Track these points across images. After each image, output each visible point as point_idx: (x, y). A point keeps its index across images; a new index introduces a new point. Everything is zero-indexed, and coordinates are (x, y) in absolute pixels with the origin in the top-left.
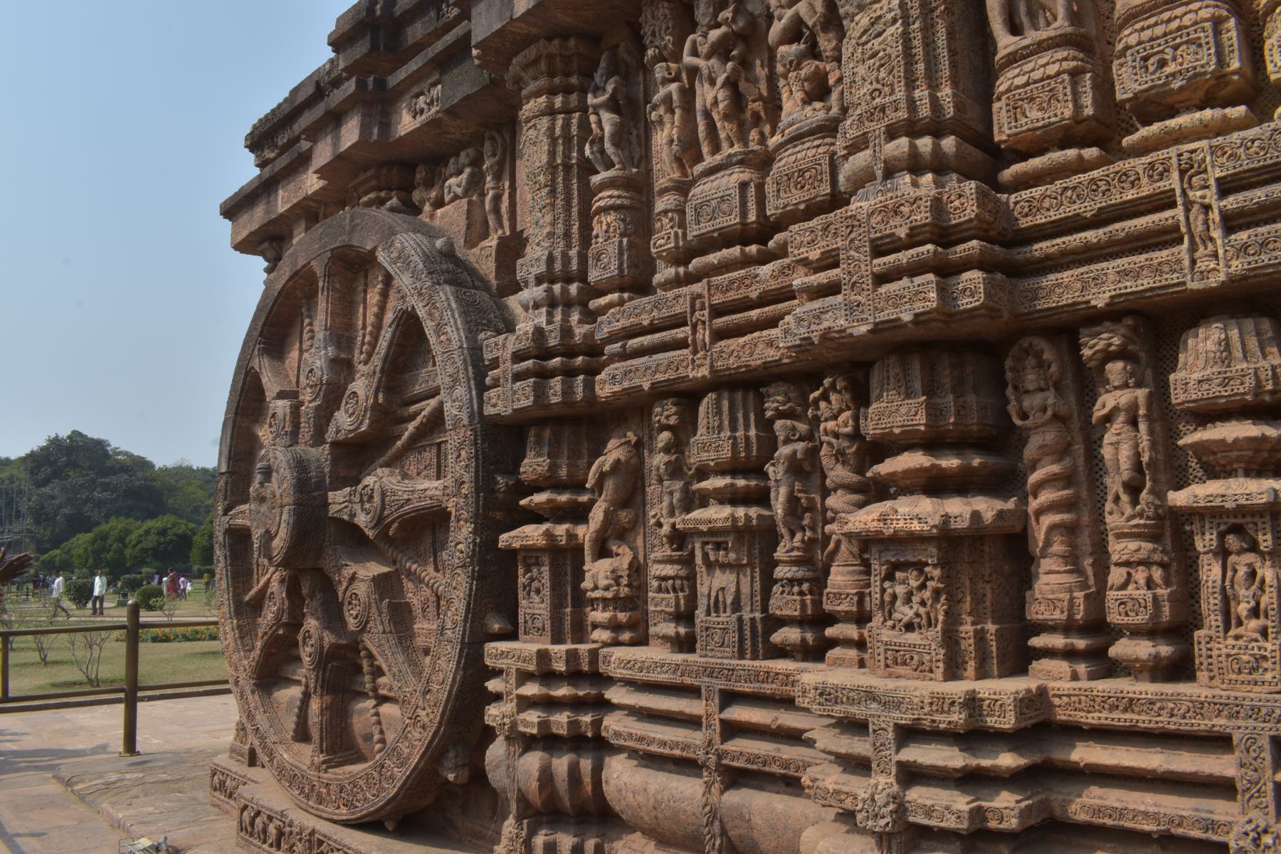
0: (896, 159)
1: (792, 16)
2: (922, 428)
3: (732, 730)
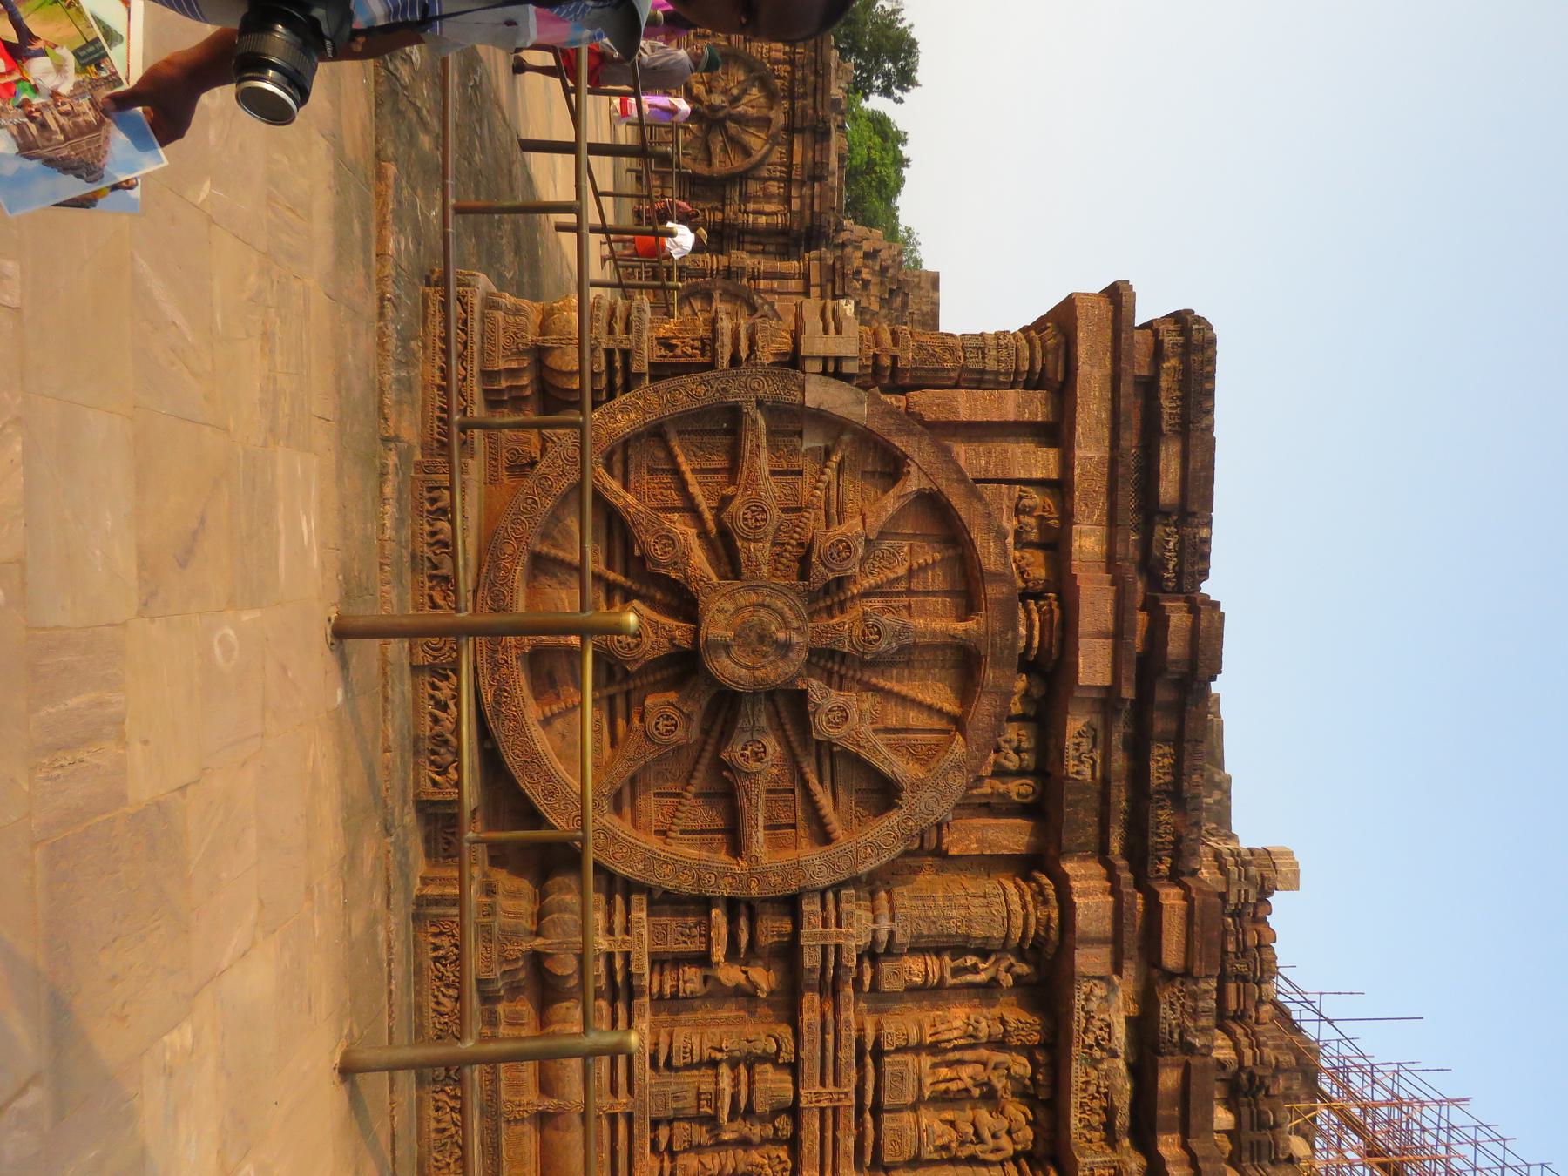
3: (613, 1119)
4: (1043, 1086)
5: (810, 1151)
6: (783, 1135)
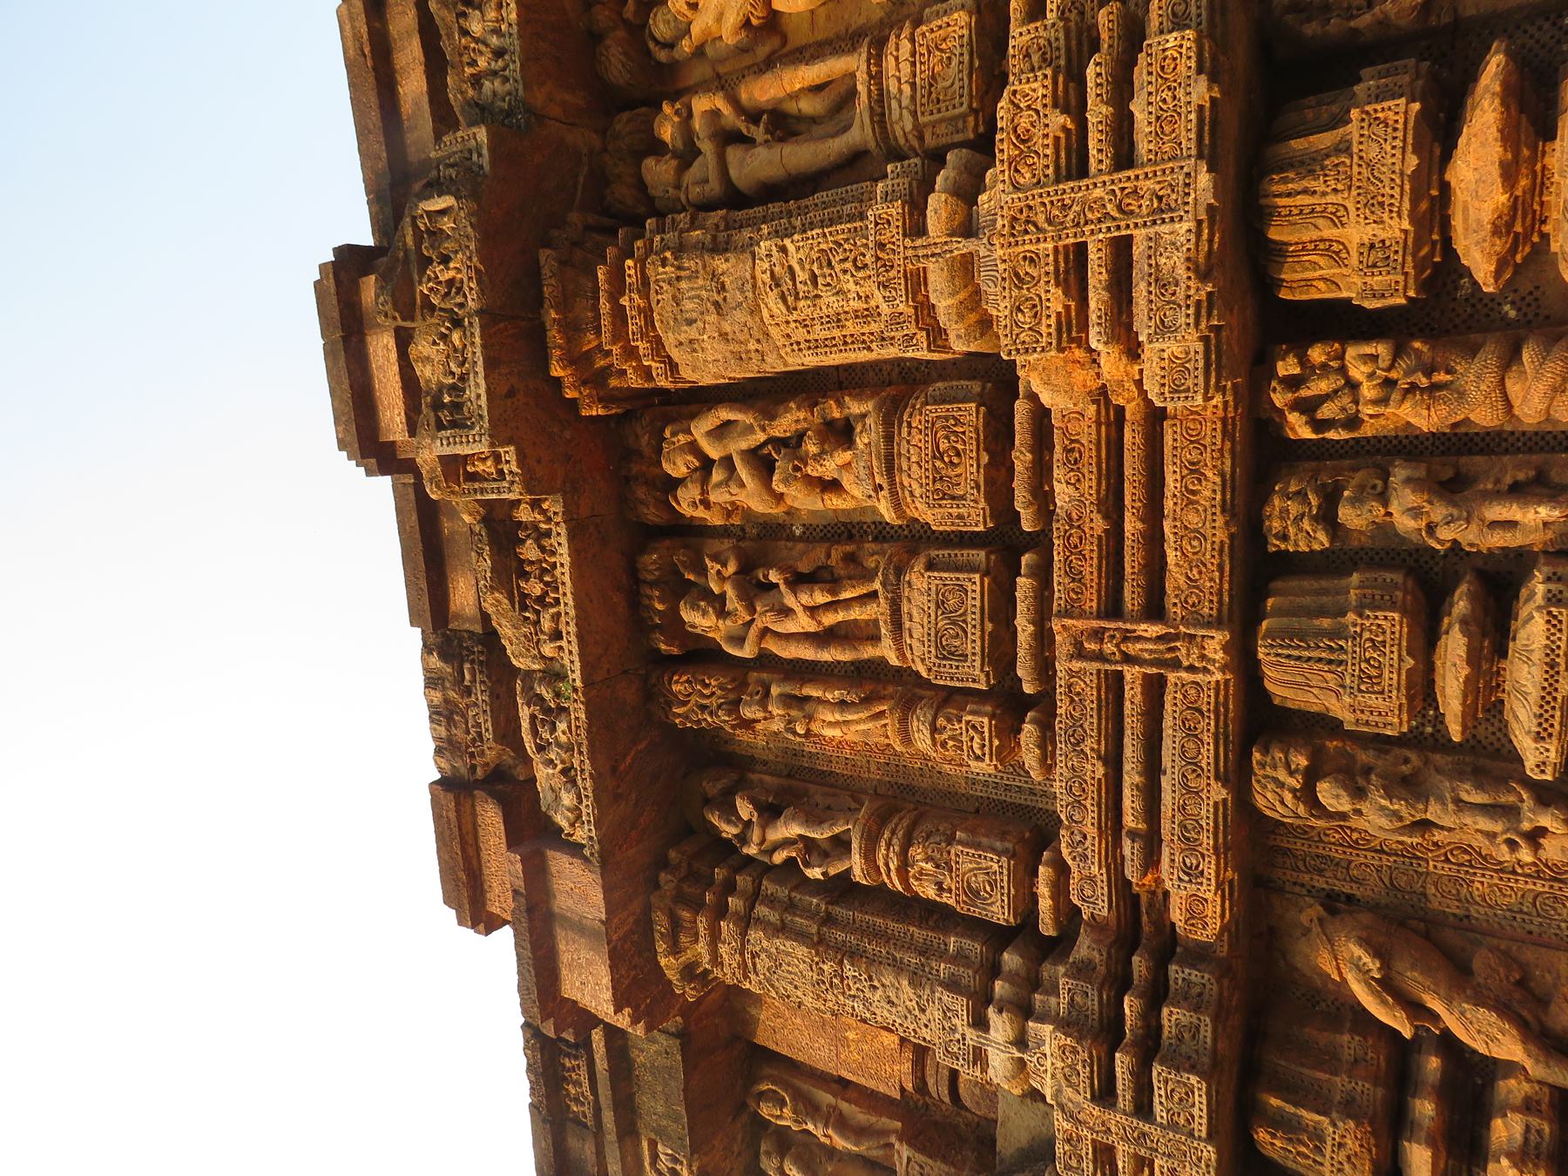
0: (951, 218)
1: (742, 459)
2: (1416, 106)
4: (652, 584)
5: (1195, 470)
6: (1301, 495)
